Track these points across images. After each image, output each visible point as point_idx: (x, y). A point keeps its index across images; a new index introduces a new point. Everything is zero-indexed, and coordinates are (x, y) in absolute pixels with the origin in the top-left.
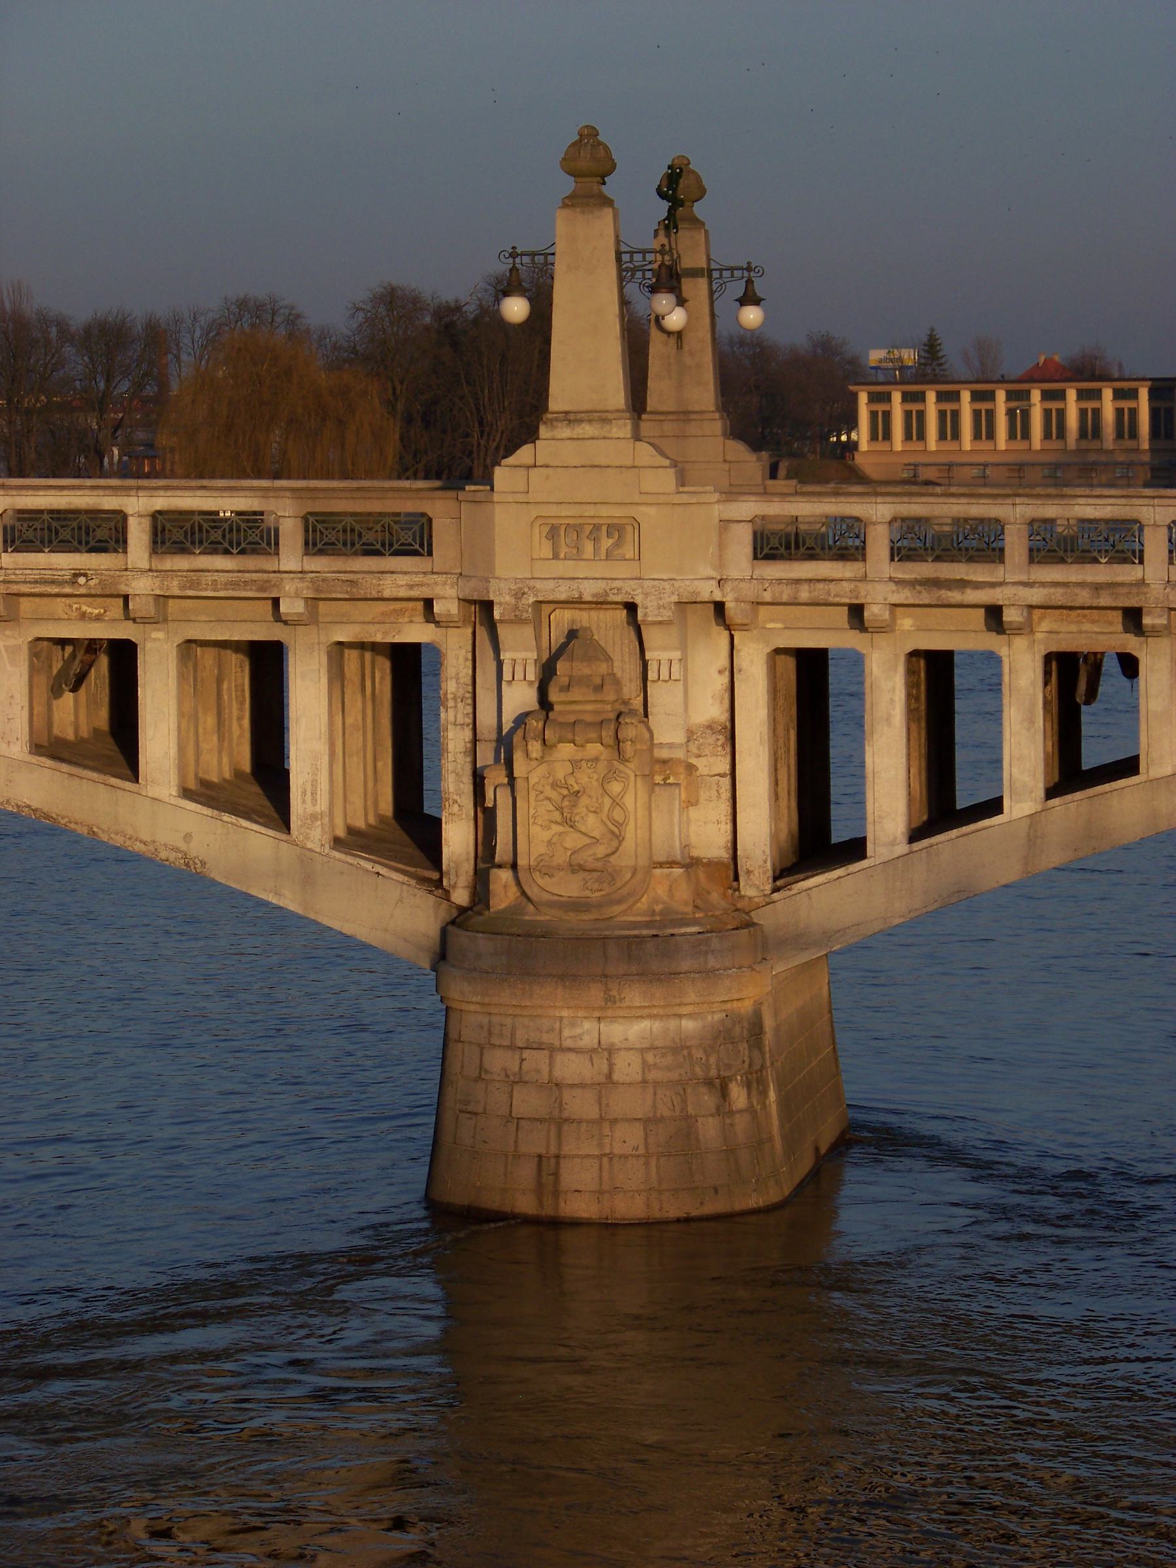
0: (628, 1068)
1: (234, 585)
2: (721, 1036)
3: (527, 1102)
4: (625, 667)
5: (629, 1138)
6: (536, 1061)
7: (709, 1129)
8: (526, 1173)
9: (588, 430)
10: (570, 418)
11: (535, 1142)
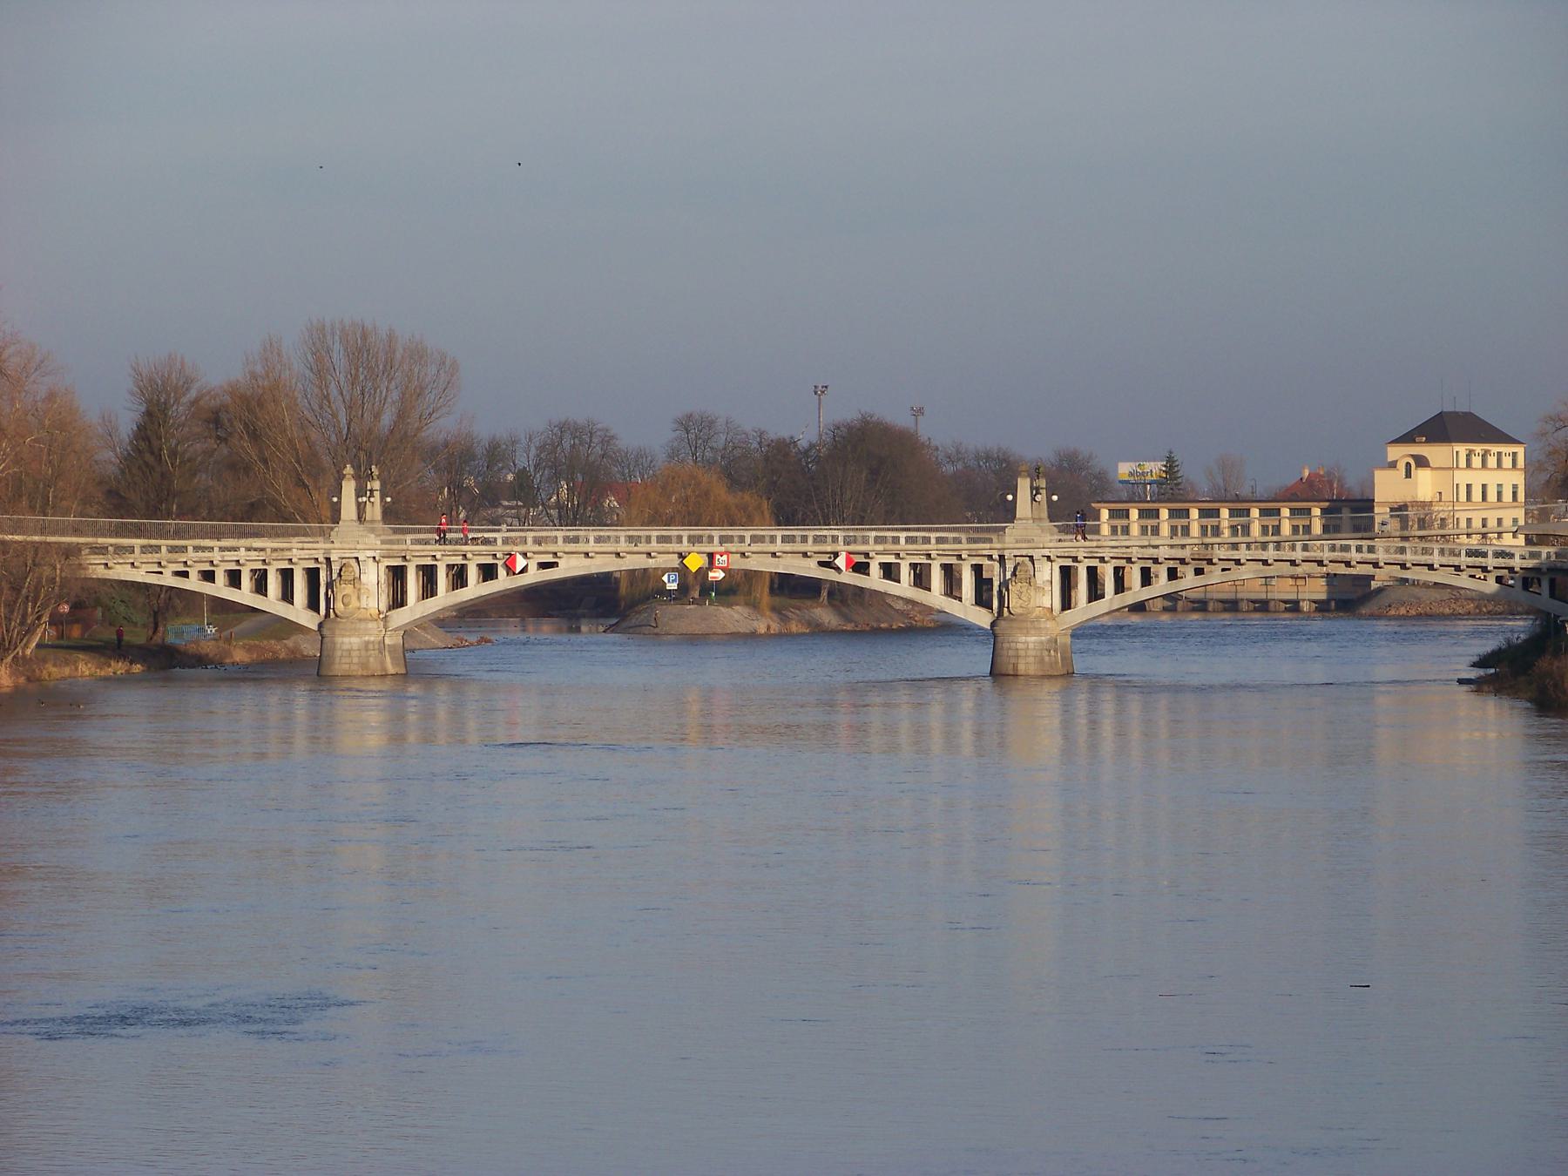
2: (1049, 641)
3: (1011, 653)
5: (1031, 660)
6: (1013, 645)
7: (1047, 659)
8: (1011, 666)
9: (1024, 521)
10: (1020, 519)
11: (1013, 661)
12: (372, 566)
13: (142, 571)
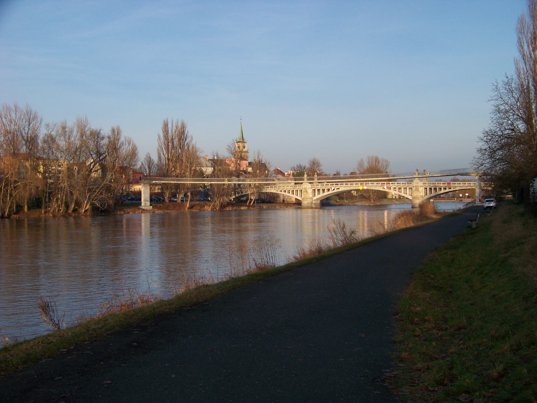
0: (418, 202)
12: (310, 189)
13: (275, 191)
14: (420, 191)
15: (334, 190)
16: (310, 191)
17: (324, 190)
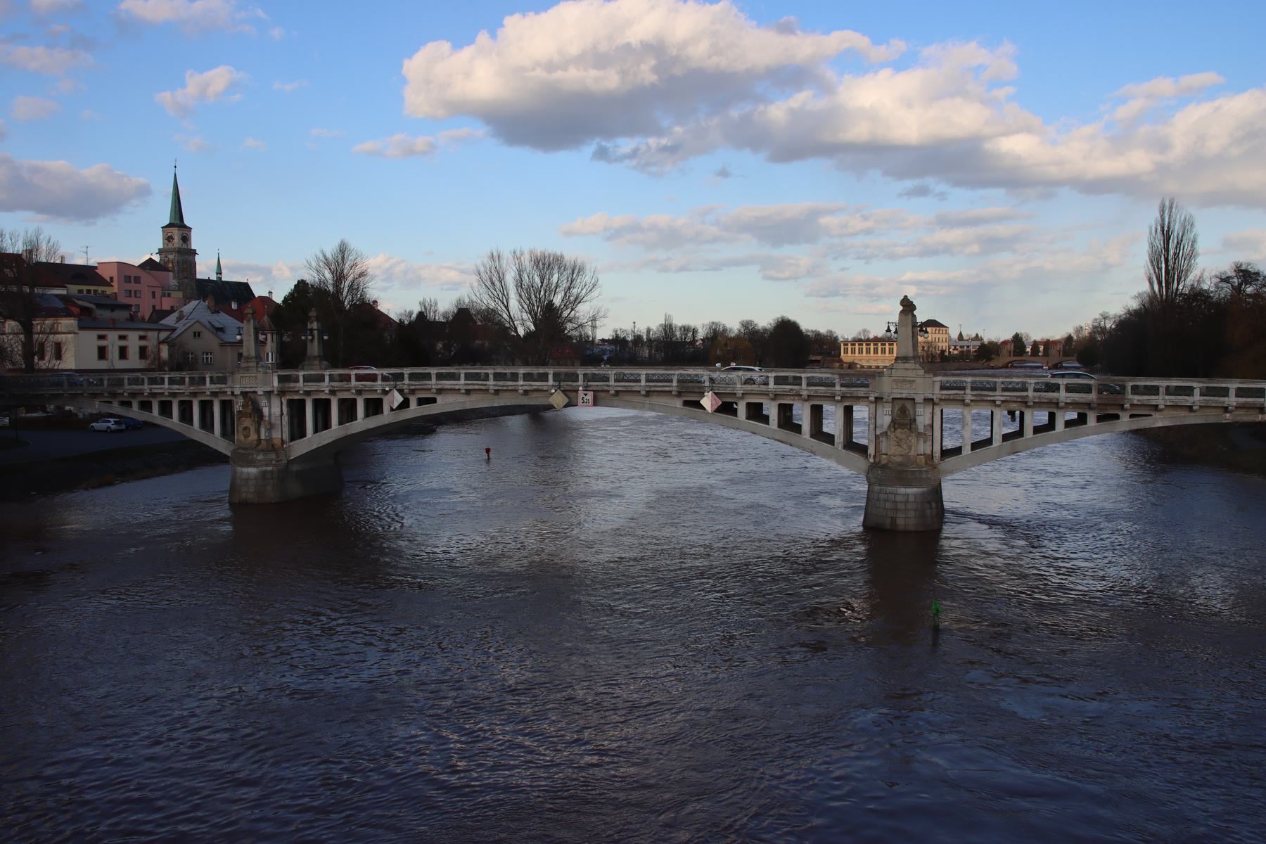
0: (911, 499)
1: (824, 393)
4: (911, 412)
5: (912, 514)
7: (928, 512)
14: (921, 429)
15: (405, 404)
16: (275, 410)
17: (348, 411)
